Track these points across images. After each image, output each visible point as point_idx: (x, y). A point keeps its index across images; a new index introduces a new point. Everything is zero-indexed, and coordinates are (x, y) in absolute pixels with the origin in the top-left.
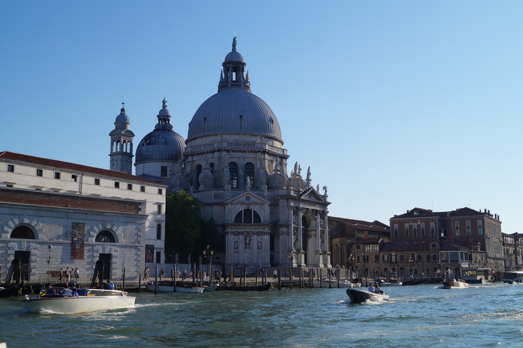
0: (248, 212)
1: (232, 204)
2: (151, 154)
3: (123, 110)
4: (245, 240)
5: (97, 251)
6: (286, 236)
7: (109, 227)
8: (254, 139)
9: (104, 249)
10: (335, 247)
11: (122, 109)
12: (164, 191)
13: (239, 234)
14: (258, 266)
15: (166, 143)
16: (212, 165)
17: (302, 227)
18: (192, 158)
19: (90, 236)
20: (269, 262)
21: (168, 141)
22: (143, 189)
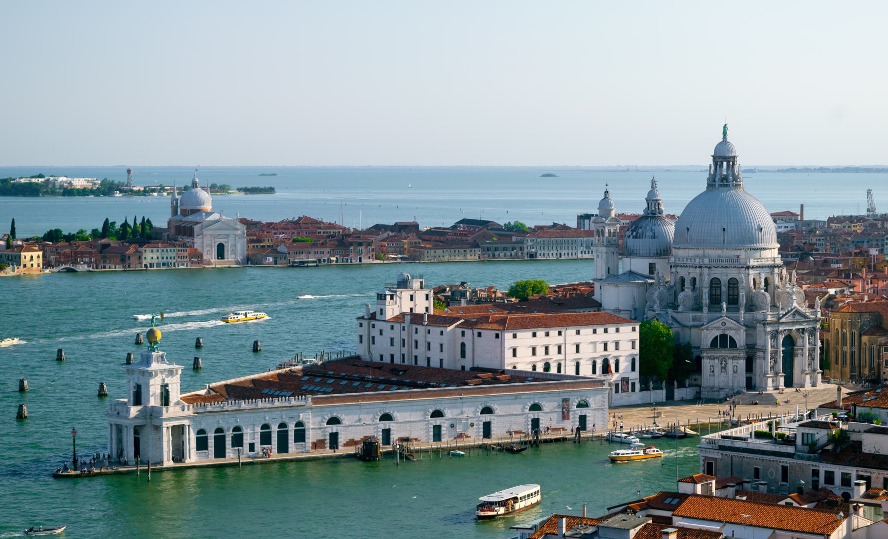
0: (724, 337)
1: (707, 329)
2: (638, 249)
3: (606, 192)
4: (721, 363)
5: (577, 414)
6: (762, 360)
7: (584, 398)
8: (738, 253)
9: (581, 412)
10: (863, 346)
11: (605, 192)
12: (637, 328)
13: (714, 358)
14: (733, 389)
15: (654, 237)
16: (694, 280)
17: (782, 349)
18: (676, 269)
19: (573, 405)
20: (745, 385)
21: (656, 234)
22: (617, 330)
